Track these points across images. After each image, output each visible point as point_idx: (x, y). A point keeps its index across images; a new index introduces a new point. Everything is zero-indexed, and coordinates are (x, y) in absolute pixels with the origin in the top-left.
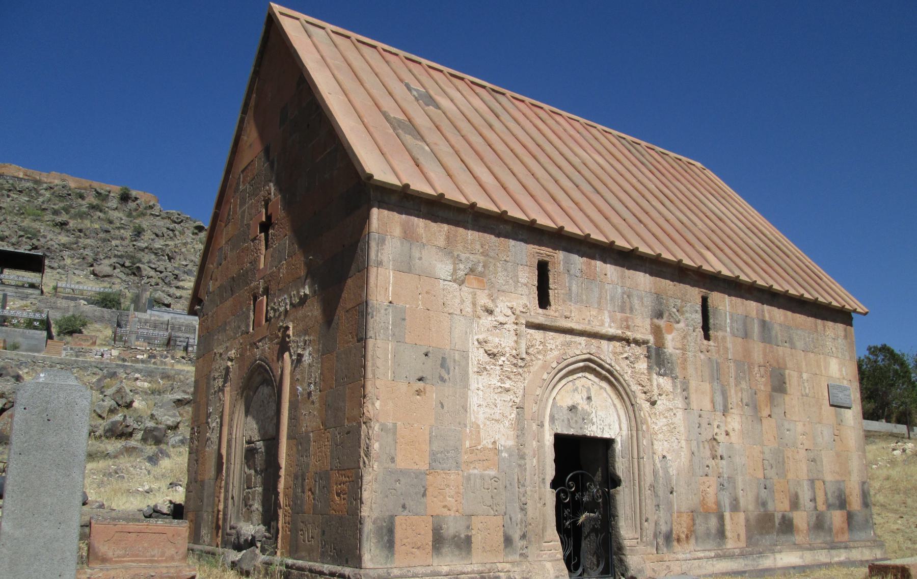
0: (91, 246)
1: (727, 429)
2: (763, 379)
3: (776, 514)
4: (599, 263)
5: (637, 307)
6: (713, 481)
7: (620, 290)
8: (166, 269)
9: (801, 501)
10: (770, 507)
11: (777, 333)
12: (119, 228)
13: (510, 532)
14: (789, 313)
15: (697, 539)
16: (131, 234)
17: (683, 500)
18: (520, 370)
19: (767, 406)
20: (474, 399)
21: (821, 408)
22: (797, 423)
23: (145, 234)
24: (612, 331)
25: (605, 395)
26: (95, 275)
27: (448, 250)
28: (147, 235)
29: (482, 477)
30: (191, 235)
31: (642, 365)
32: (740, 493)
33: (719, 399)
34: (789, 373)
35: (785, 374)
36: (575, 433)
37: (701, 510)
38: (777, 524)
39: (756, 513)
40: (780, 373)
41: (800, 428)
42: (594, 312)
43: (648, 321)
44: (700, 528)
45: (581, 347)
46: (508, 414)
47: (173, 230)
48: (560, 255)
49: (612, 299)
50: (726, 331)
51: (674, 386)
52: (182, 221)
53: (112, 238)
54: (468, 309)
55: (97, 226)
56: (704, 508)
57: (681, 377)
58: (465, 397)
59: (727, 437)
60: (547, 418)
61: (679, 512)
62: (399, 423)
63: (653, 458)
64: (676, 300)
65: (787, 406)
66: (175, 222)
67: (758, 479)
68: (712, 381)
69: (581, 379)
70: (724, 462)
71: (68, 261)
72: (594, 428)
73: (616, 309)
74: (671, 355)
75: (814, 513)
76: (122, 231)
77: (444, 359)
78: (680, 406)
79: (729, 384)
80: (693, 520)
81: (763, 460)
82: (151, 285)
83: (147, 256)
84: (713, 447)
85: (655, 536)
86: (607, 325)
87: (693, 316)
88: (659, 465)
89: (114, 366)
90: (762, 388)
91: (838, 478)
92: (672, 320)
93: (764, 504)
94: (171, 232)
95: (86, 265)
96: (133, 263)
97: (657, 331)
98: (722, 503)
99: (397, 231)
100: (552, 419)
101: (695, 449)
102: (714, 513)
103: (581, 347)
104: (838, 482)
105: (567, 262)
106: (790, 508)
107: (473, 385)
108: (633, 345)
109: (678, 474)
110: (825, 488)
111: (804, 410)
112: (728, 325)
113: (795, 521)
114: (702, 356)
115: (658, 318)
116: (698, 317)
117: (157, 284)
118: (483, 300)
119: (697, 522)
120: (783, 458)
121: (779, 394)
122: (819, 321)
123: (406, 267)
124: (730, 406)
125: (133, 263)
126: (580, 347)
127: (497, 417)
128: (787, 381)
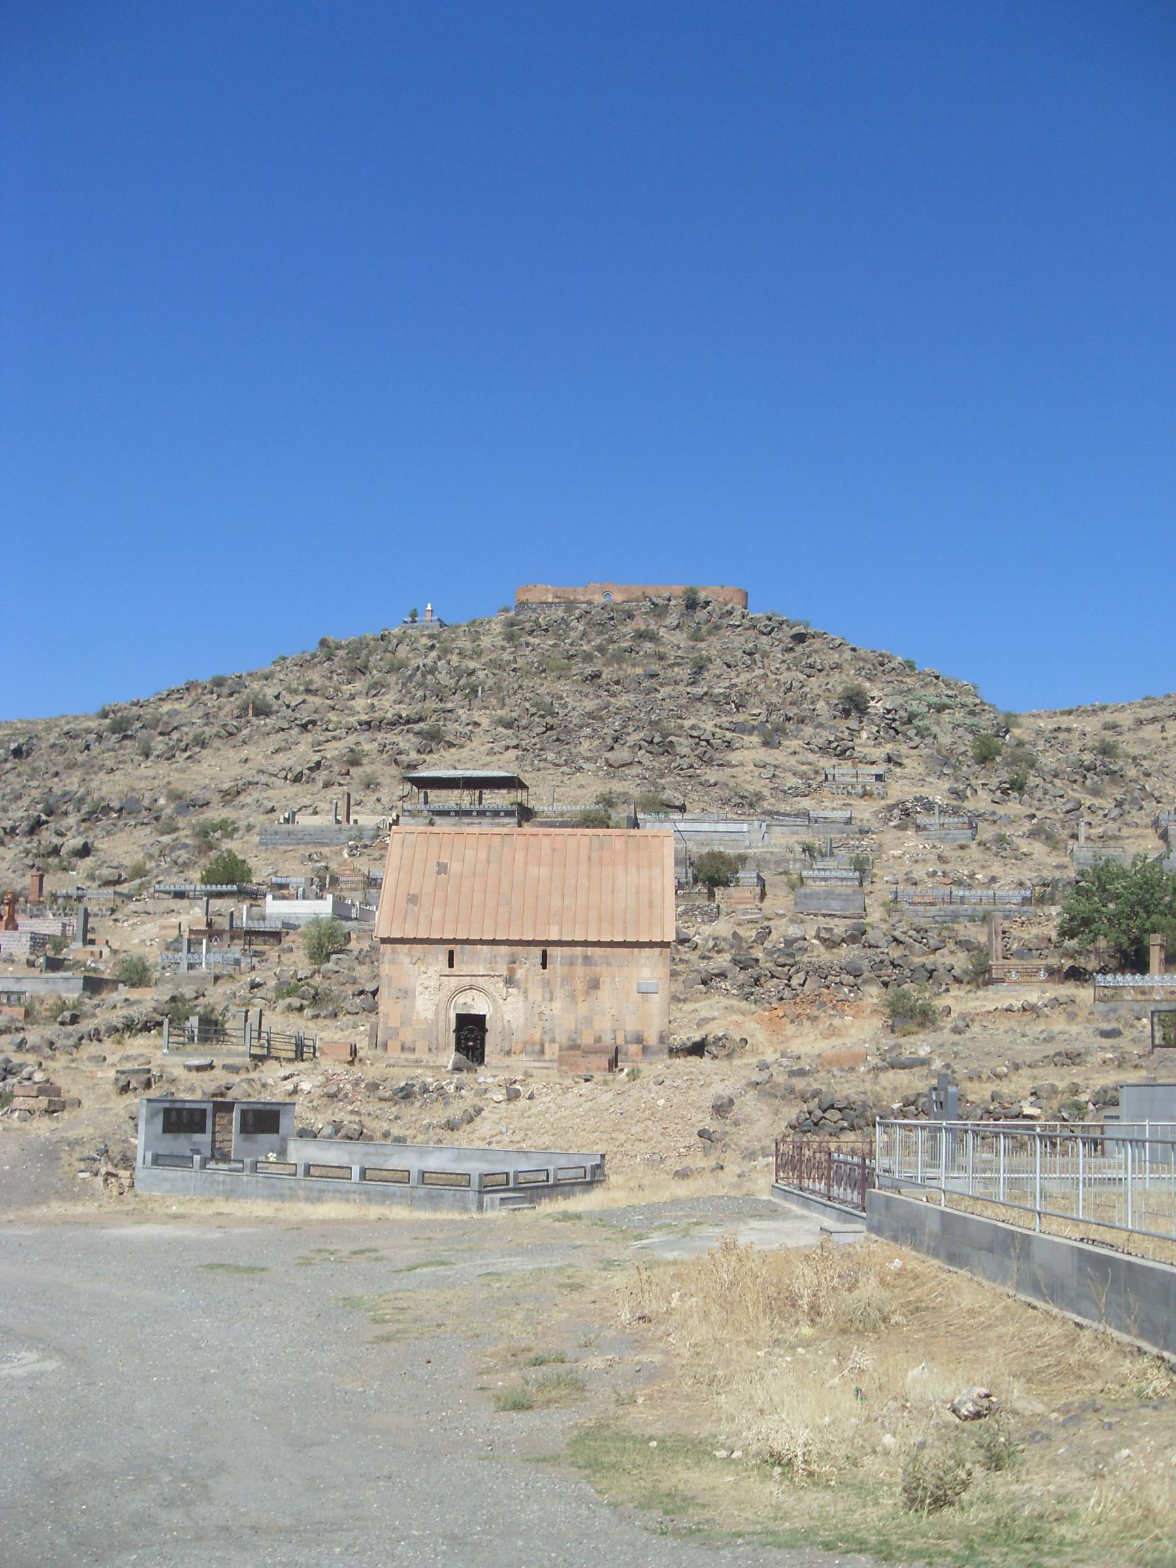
0: (626, 707)
8: (713, 735)
10: (579, 1042)
12: (671, 666)
16: (689, 671)
23: (710, 666)
24: (482, 973)
26: (610, 766)
27: (409, 954)
28: (716, 668)
30: (780, 656)
31: (501, 984)
33: (547, 995)
42: (473, 967)
44: (529, 1048)
45: (467, 981)
47: (749, 654)
48: (459, 946)
51: (519, 992)
52: (773, 629)
53: (662, 685)
54: (417, 973)
55: (639, 671)
57: (523, 987)
66: (765, 634)
71: (586, 745)
76: (676, 669)
82: (682, 769)
83: (704, 707)
94: (747, 657)
95: (604, 749)
96: (664, 737)
99: (390, 951)
100: (455, 1008)
101: (528, 1016)
103: (467, 981)
107: (418, 998)
116: (540, 960)
117: (691, 767)
118: (423, 969)
122: (636, 950)
123: (392, 962)
125: (664, 737)
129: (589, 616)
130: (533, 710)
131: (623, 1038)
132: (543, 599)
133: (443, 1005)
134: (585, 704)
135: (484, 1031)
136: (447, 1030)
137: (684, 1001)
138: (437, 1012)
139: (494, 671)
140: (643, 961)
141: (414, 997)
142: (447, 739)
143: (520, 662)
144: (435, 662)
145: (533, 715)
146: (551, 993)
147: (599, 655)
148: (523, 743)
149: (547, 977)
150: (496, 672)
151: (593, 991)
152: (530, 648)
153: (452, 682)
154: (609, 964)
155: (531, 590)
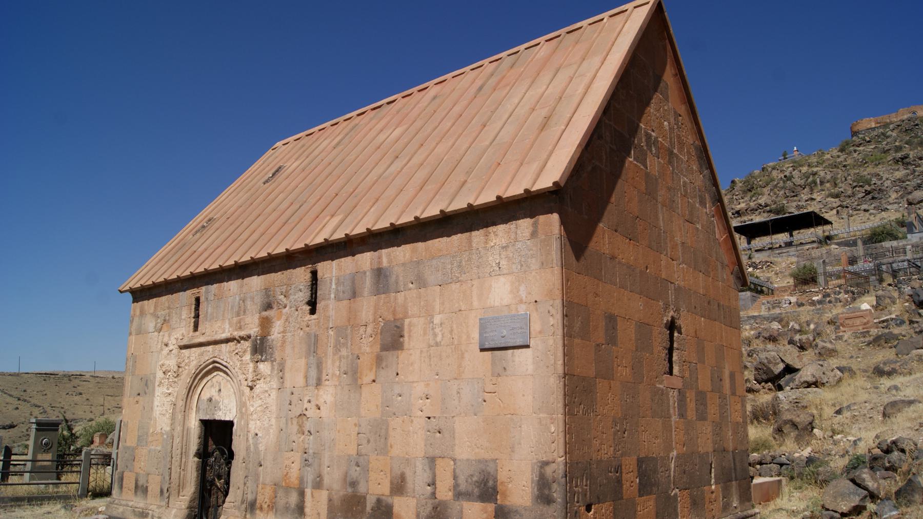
1: (318, 403)
2: (371, 339)
3: (368, 496)
4: (225, 283)
5: (249, 307)
6: (297, 457)
7: (238, 299)
9: (410, 485)
10: (362, 489)
11: (397, 276)
13: (163, 487)
14: (420, 245)
15: (276, 511)
17: (268, 473)
18: (176, 380)
19: (371, 370)
20: (156, 403)
21: (463, 358)
22: (415, 385)
24: (224, 336)
25: (230, 386)
29: (155, 450)
31: (248, 357)
32: (326, 471)
33: (313, 373)
34: (410, 325)
35: (403, 325)
36: (210, 419)
37: (284, 484)
38: (368, 508)
39: (341, 493)
40: (396, 326)
41: (420, 389)
43: (257, 316)
44: (281, 502)
46: (168, 410)
48: (204, 288)
49: (232, 308)
50: (329, 299)
51: (273, 369)
56: (286, 483)
57: (278, 359)
58: (153, 402)
59: (318, 411)
60: (195, 409)
61: (264, 484)
62: (129, 421)
63: (247, 435)
64: (282, 287)
65: (400, 366)
67: (349, 456)
68: (308, 355)
69: (216, 377)
70: (311, 437)
72: (220, 413)
73: (234, 315)
74: (273, 340)
75: (430, 502)
77: (147, 380)
78: (275, 387)
79: (326, 355)
80: (275, 492)
81: (358, 434)
84: (303, 423)
85: (242, 502)
86: (227, 331)
87: (296, 297)
88: (251, 441)
89: (746, 318)
90: (368, 350)
91: (487, 456)
92: (281, 307)
93: (354, 484)
97: (266, 324)
98: (305, 480)
99: (138, 313)
101: (283, 426)
102: (295, 488)
104: (480, 461)
105: (207, 292)
106: (391, 492)
108: (242, 342)
109: (266, 450)
110: (454, 470)
111: (431, 365)
112: (333, 291)
113: (396, 509)
114: (302, 333)
115: (266, 310)
116: (304, 295)
119: (278, 495)
120: (387, 430)
121: (391, 352)
124: (324, 377)
126: (209, 354)
127: (164, 412)
128: (406, 334)
129: (900, 128)
130: (855, 184)
131: (450, 482)
132: (869, 126)
133: (181, 403)
134: (896, 175)
135: (231, 455)
136: (184, 453)
137: (889, 374)
138: (173, 418)
139: (831, 170)
140: (492, 259)
141: (154, 390)
142: (790, 211)
143: (849, 162)
144: (791, 173)
145: (855, 187)
146: (319, 367)
147: (907, 146)
148: (845, 203)
149: (314, 329)
150: (831, 170)
151: (390, 356)
152: (857, 153)
153: (803, 182)
154: (421, 282)
155: (859, 123)
